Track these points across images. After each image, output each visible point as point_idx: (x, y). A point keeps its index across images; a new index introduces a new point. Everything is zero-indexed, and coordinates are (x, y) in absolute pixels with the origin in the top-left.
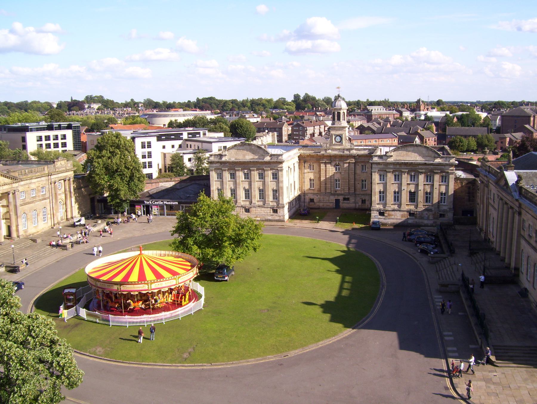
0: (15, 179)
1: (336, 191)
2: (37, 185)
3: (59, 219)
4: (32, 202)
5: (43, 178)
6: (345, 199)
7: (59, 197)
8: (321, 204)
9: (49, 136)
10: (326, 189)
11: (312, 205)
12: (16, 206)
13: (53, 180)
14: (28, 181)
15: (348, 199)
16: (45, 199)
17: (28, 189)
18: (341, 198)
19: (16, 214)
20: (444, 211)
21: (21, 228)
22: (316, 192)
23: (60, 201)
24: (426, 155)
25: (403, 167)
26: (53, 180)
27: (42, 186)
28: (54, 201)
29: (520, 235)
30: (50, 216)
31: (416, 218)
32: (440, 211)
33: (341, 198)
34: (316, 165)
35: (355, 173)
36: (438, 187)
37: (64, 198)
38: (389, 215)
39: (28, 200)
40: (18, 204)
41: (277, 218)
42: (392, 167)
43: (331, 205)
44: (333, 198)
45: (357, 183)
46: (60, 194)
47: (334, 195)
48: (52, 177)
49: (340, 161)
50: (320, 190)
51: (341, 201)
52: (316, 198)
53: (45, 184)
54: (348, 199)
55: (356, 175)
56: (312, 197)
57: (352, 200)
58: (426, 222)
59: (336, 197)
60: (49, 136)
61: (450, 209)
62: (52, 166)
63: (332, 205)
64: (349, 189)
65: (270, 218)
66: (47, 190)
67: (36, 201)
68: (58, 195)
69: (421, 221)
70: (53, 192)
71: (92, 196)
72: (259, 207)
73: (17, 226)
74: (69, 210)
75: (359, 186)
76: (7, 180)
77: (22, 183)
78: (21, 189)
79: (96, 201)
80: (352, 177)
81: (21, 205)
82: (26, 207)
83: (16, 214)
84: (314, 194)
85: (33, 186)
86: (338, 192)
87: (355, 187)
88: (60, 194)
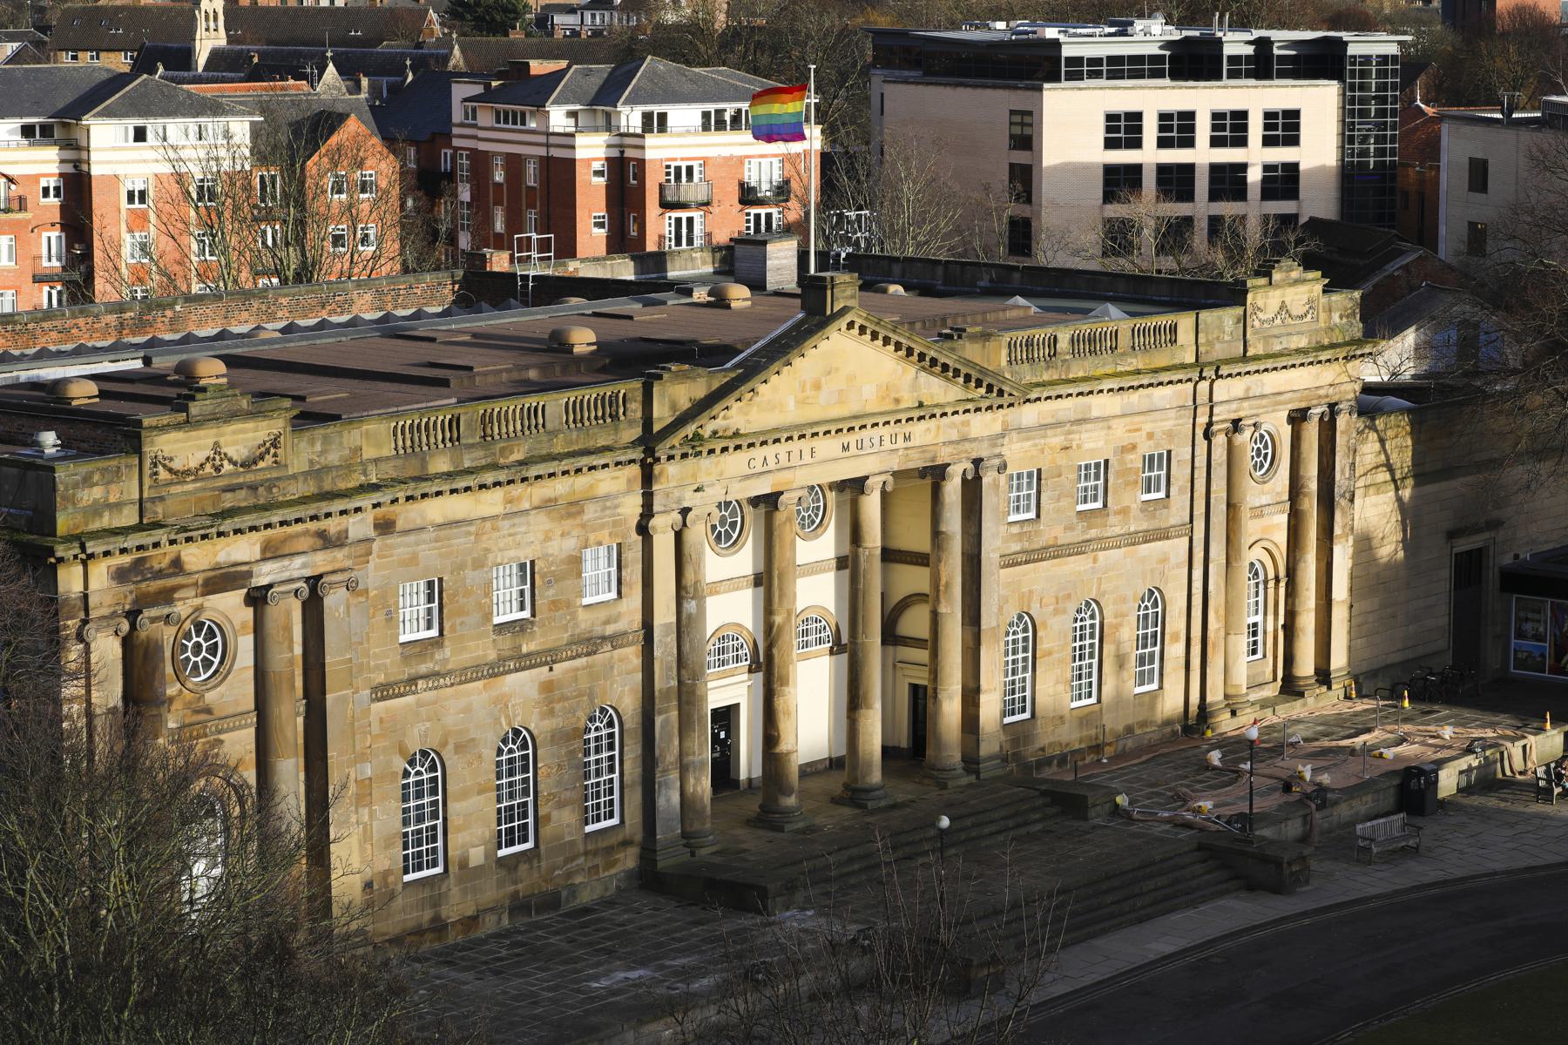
0: (991, 389)
3: (1241, 676)
4: (1077, 549)
7: (1251, 528)
9: (1242, 116)
13: (1223, 414)
14: (1066, 408)
16: (1163, 535)
17: (1062, 460)
23: (1257, 554)
26: (1223, 414)
27: (1146, 448)
37: (1281, 537)
40: (994, 544)
46: (1259, 512)
48: (1223, 390)
53: (1170, 435)
60: (1242, 116)
62: (1226, 318)
66: (1180, 474)
67: (1105, 543)
68: (1245, 514)
71: (1465, 545)
74: (1307, 622)
76: (938, 390)
77: (1029, 414)
79: (1492, 578)
81: (1010, 562)
88: (1259, 512)
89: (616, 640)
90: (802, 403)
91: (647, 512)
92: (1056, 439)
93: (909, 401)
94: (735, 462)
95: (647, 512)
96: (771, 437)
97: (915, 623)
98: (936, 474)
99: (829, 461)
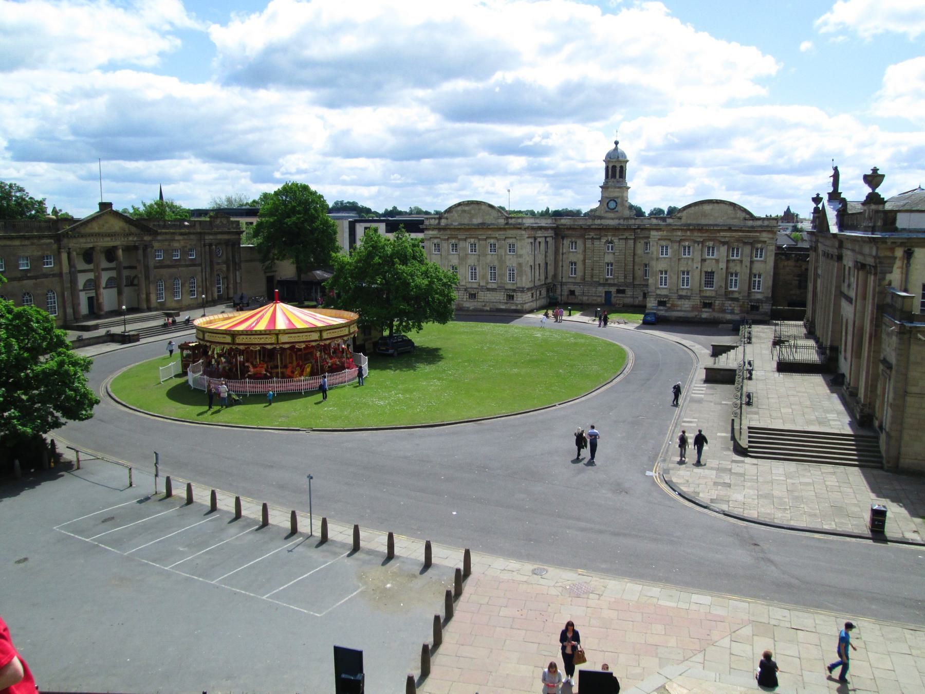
1: (607, 280)
2: (182, 243)
5: (192, 237)
6: (619, 291)
7: (216, 267)
8: (585, 298)
10: (592, 276)
11: (572, 300)
12: (147, 268)
13: (207, 241)
14: (168, 237)
15: (623, 292)
16: (194, 265)
18: (613, 290)
19: (147, 277)
20: (758, 301)
21: (153, 297)
22: (578, 281)
24: (732, 216)
25: (696, 234)
26: (207, 241)
27: (189, 247)
28: (208, 270)
29: (841, 294)
30: (200, 289)
31: (714, 310)
32: (751, 301)
33: (613, 290)
34: (580, 242)
35: (634, 255)
36: (748, 265)
37: (225, 269)
38: (673, 305)
39: (168, 263)
40: (151, 264)
41: (513, 307)
42: (679, 233)
43: (599, 300)
44: (601, 290)
45: (636, 268)
47: (604, 285)
48: (207, 237)
49: (614, 235)
50: (584, 278)
51: (614, 295)
52: (578, 290)
54: (623, 292)
55: (636, 257)
56: (572, 288)
57: (629, 292)
58: (729, 317)
59: (607, 289)
61: (767, 298)
63: (601, 300)
64: (625, 277)
65: (503, 307)
69: (721, 315)
70: (208, 256)
71: (269, 274)
72: (488, 290)
73: (148, 295)
74: (231, 286)
75: (639, 273)
77: (159, 238)
78: (156, 245)
80: (630, 259)
81: (156, 267)
82: (164, 271)
83: (147, 277)
84: (575, 284)
85: (176, 245)
86: (609, 282)
87: (634, 274)
88: (218, 264)
89: (54, 275)
90: (99, 228)
91: (59, 248)
92: (167, 243)
93: (127, 231)
94: (83, 240)
95: (59, 248)
96: (92, 235)
97: (136, 282)
98: (135, 248)
99: (108, 243)
